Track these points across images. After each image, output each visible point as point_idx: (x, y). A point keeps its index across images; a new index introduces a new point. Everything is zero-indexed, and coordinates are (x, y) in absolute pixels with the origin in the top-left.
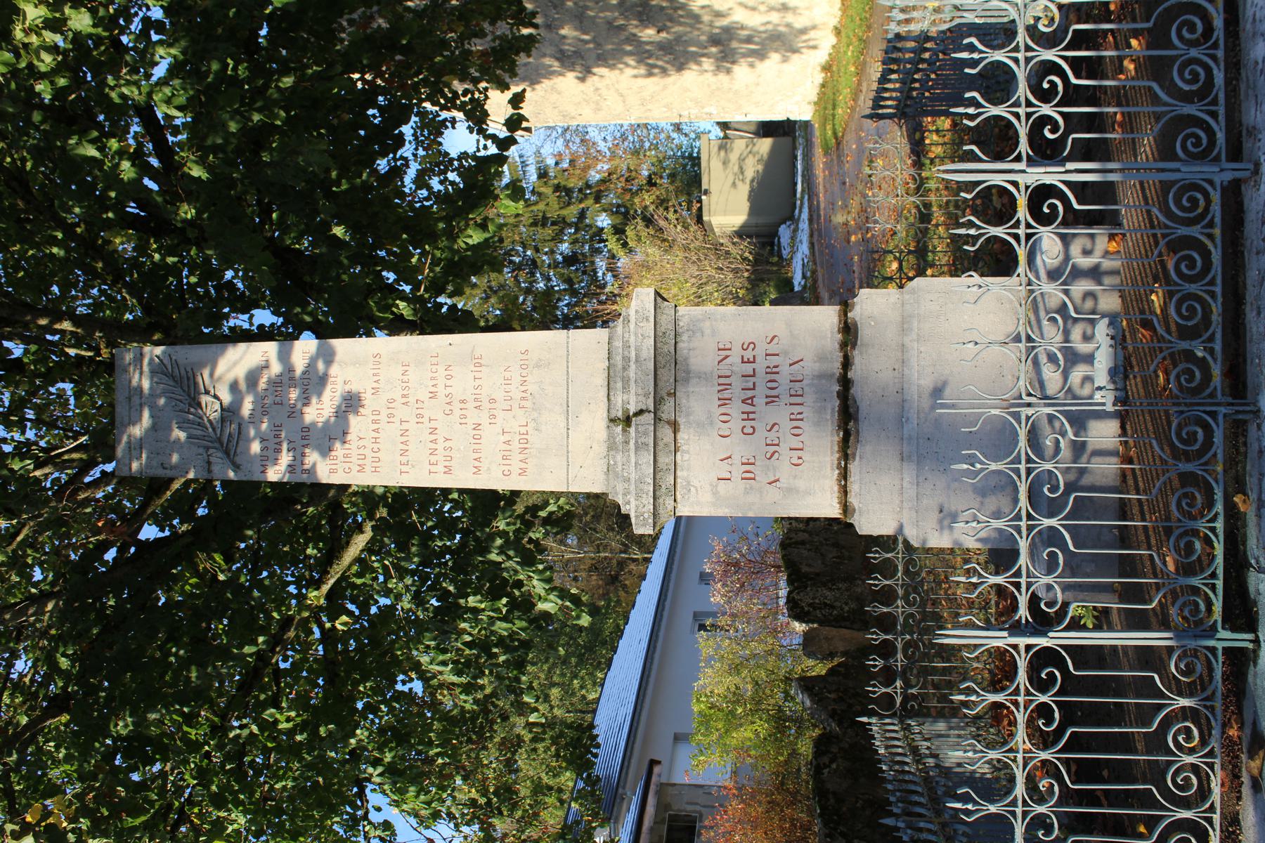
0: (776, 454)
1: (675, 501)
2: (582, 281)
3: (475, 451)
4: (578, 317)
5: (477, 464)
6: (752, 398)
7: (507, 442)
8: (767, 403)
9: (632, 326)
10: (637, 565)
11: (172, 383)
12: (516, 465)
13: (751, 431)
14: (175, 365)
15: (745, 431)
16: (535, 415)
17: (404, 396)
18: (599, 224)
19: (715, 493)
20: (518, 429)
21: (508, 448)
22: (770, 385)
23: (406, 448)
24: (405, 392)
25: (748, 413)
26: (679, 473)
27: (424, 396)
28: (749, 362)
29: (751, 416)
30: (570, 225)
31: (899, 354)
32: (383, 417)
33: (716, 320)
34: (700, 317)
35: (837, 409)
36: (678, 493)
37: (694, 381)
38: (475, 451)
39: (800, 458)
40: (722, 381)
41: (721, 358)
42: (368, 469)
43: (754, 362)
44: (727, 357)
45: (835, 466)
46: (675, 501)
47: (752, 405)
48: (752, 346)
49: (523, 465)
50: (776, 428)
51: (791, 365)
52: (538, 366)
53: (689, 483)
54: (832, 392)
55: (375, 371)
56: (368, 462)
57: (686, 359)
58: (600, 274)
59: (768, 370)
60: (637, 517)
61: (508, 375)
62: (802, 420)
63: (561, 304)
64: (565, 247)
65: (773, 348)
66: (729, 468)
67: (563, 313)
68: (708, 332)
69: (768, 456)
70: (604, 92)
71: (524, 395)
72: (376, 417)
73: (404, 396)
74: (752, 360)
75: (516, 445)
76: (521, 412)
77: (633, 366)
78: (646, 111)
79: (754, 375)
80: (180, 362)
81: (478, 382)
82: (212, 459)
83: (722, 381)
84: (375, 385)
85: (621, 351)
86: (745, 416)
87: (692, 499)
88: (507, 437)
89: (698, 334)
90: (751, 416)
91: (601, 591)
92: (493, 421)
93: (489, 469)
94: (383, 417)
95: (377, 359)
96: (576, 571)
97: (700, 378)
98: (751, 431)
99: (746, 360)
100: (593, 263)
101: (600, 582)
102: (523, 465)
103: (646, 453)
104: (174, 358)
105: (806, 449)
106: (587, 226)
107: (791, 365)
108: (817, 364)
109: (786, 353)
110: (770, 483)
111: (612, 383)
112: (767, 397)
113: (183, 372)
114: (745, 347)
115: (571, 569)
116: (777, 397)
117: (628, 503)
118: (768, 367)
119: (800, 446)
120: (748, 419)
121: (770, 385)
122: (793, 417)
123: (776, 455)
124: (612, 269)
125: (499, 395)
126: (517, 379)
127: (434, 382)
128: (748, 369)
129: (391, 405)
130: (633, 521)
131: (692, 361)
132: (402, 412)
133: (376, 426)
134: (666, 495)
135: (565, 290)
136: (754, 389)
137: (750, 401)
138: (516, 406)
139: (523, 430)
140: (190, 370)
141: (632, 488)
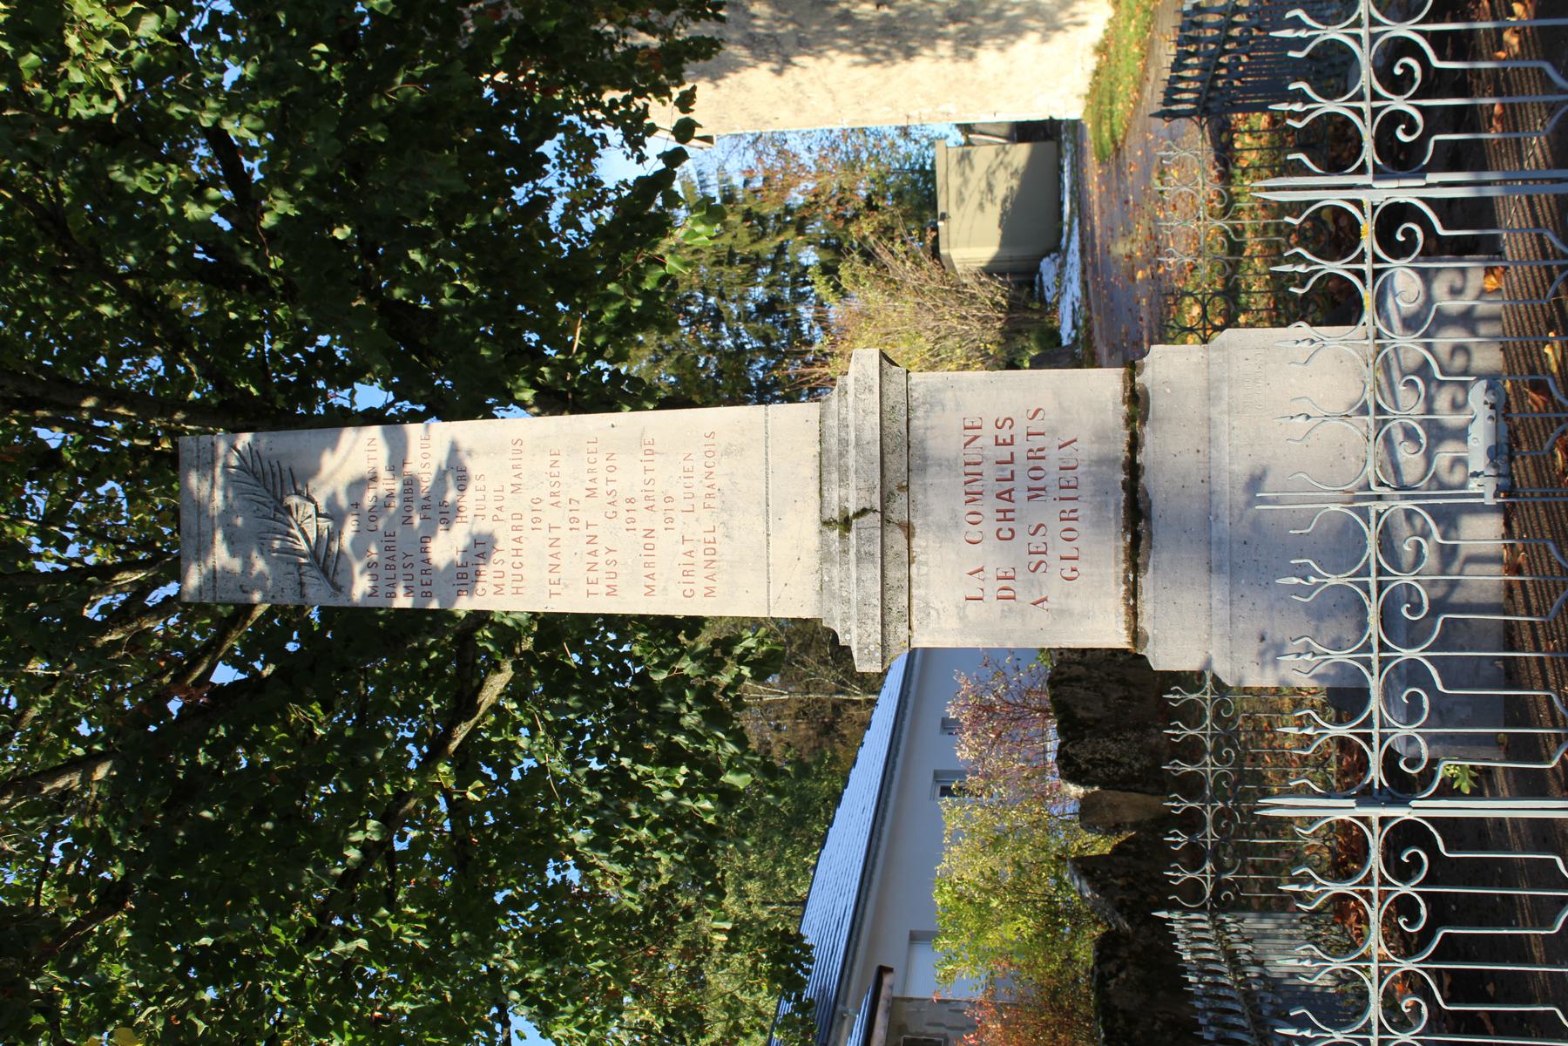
0: (1043, 565)
1: (910, 628)
2: (783, 337)
3: (647, 565)
4: (777, 383)
5: (649, 582)
6: (1010, 491)
7: (689, 553)
8: (1029, 498)
9: (850, 398)
10: (859, 709)
11: (252, 481)
12: (700, 583)
13: (1009, 534)
14: (256, 458)
15: (1002, 534)
16: (725, 516)
17: (553, 494)
18: (804, 261)
19: (962, 618)
20: (702, 536)
21: (690, 560)
23: (556, 562)
24: (555, 489)
25: (1004, 511)
26: (914, 592)
27: (580, 494)
28: (1005, 444)
29: (1009, 515)
30: (765, 264)
31: (1205, 430)
32: (526, 522)
33: (960, 389)
34: (940, 386)
35: (1122, 504)
36: (913, 618)
37: (932, 470)
38: (647, 565)
39: (1074, 570)
40: (970, 469)
41: (968, 439)
42: (508, 590)
43: (1012, 444)
44: (976, 437)
45: (1121, 580)
46: (910, 628)
47: (1010, 500)
48: (1009, 423)
49: (711, 583)
50: (1042, 530)
51: (1060, 447)
52: (727, 453)
53: (927, 604)
55: (515, 462)
56: (507, 581)
57: (922, 442)
58: (805, 327)
59: (1031, 454)
60: (860, 650)
61: (688, 465)
62: (1076, 519)
63: (755, 367)
64: (759, 292)
65: (1036, 426)
67: (757, 379)
68: (950, 405)
69: (1032, 568)
71: (710, 491)
72: (517, 523)
73: (553, 494)
74: (1008, 441)
75: (700, 557)
76: (707, 513)
79: (1012, 462)
81: (650, 475)
82: (306, 579)
83: (970, 469)
84: (516, 481)
85: (836, 431)
86: (1001, 515)
88: (688, 547)
89: (938, 409)
90: (1009, 515)
91: (811, 744)
92: (669, 526)
93: (665, 589)
94: (526, 522)
95: (517, 447)
96: (778, 717)
97: (940, 465)
99: (1001, 441)
100: (794, 311)
101: (811, 732)
102: (711, 583)
103: (871, 565)
106: (787, 264)
107: (1060, 447)
108: (1096, 446)
109: (1054, 431)
110: (1034, 604)
111: (825, 474)
112: (1029, 490)
114: (1000, 424)
115: (772, 715)
116: (1043, 489)
117: (848, 631)
118: (1030, 450)
119: (1075, 554)
120: (1005, 519)
122: (1064, 515)
124: (821, 320)
125: (678, 492)
126: (700, 471)
127: (592, 476)
128: (1004, 453)
129: (536, 507)
130: (855, 655)
131: (930, 444)
132: (550, 516)
133: (517, 534)
134: (899, 620)
135: (759, 349)
136: (1012, 479)
137: (1007, 496)
138: (699, 505)
139: (709, 537)
140: (274, 463)
141: (854, 611)
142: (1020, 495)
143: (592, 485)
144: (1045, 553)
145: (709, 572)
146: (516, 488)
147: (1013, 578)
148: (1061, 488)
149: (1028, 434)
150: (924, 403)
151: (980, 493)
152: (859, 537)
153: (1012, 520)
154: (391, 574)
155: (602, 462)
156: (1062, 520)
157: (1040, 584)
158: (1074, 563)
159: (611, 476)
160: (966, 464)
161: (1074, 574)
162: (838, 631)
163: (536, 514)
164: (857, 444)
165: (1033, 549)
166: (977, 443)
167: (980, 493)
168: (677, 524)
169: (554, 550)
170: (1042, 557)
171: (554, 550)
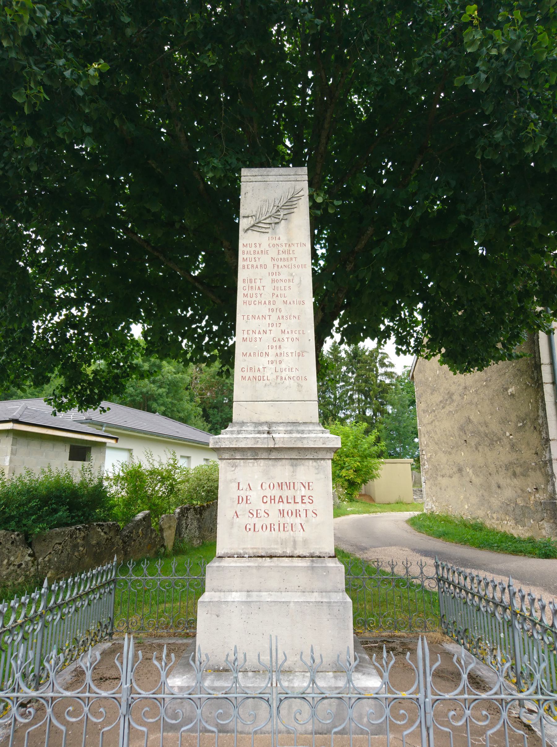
0: (252, 516)
3: (254, 353)
5: (248, 354)
6: (283, 501)
7: (259, 370)
8: (280, 510)
9: (321, 435)
11: (289, 197)
12: (248, 374)
13: (265, 501)
14: (298, 198)
15: (265, 498)
16: (273, 384)
17: (283, 317)
19: (231, 481)
20: (266, 375)
21: (256, 370)
22: (290, 512)
23: (256, 318)
24: (285, 317)
25: (274, 499)
26: (242, 461)
27: (283, 327)
28: (302, 500)
29: (273, 501)
31: (308, 590)
32: (272, 306)
35: (277, 551)
37: (291, 468)
38: (254, 353)
39: (250, 529)
40: (292, 485)
41: (304, 484)
42: (245, 299)
43: (302, 503)
44: (305, 487)
45: (245, 550)
47: (279, 502)
48: (311, 501)
49: (247, 378)
50: (266, 515)
51: (301, 524)
52: (299, 385)
53: (236, 466)
54: (286, 548)
55: (295, 302)
56: (249, 299)
59: (298, 511)
60: (219, 438)
61: (294, 370)
62: (271, 530)
65: (310, 513)
66: (245, 488)
69: (251, 511)
70: (433, 414)
71: (284, 378)
72: (272, 303)
73: (283, 317)
74: (303, 501)
75: (257, 374)
76: (275, 377)
77: (299, 435)
78: (424, 434)
79: (295, 503)
80: (300, 201)
81: (290, 355)
82: (250, 218)
83: (292, 485)
84: (288, 302)
85: (307, 429)
86: (273, 498)
87: (228, 468)
88: (262, 370)
89: (316, 471)
90: (273, 501)
92: (270, 362)
93: (245, 360)
94: (272, 306)
95: (302, 303)
97: (293, 472)
98: (265, 501)
99: (303, 498)
102: (247, 378)
103: (253, 443)
104: (302, 197)
105: (255, 533)
107: (301, 524)
108: (301, 540)
109: (307, 521)
110: (236, 512)
111: (289, 424)
112: (283, 510)
113: (295, 203)
114: (310, 498)
116: (283, 516)
117: (226, 434)
118: (299, 511)
119: (256, 530)
120: (271, 499)
121: (290, 512)
122: (272, 525)
123: (251, 516)
125: (283, 366)
126: (292, 375)
127: (290, 332)
128: (298, 500)
129: (278, 310)
130: (217, 437)
132: (274, 316)
133: (267, 303)
136: (288, 503)
137: (281, 500)
138: (278, 374)
139: (265, 378)
140: (296, 206)
141: (234, 436)
142: (281, 506)
143: (286, 332)
144: (257, 516)
145: (252, 378)
146: (285, 302)
147: (247, 502)
148: (284, 524)
149: (306, 510)
150: (319, 465)
151: (282, 489)
152: (265, 438)
153: (271, 502)
154: (252, 253)
155: (295, 336)
156: (271, 524)
157: (244, 515)
158: (252, 529)
159: (290, 340)
160: (294, 483)
161: (248, 530)
162: (227, 429)
163: (275, 310)
164: (301, 438)
165: (259, 511)
166: (303, 488)
167: (282, 489)
168: (270, 366)
169: (261, 317)
170: (255, 515)
171: (261, 317)
